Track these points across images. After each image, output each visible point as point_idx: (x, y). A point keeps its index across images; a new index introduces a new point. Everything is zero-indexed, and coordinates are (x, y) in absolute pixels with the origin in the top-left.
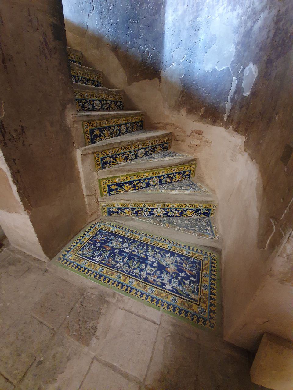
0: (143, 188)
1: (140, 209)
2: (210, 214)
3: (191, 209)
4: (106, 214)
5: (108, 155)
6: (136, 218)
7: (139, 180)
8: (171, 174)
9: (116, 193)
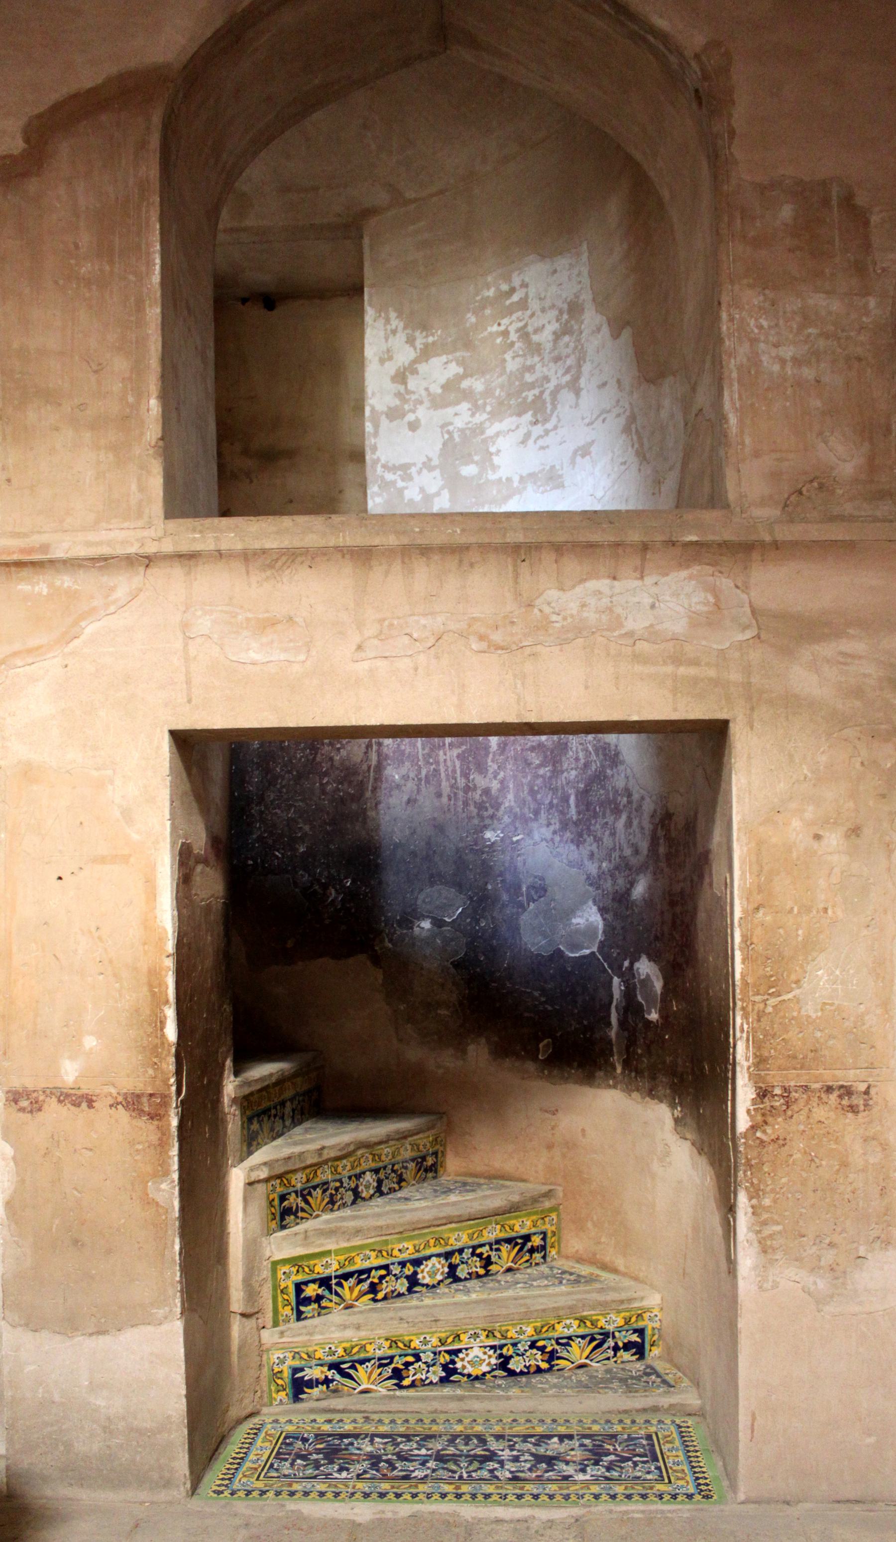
0: (400, 1295)
1: (410, 1359)
3: (583, 1337)
6: (398, 1393)
7: (386, 1267)
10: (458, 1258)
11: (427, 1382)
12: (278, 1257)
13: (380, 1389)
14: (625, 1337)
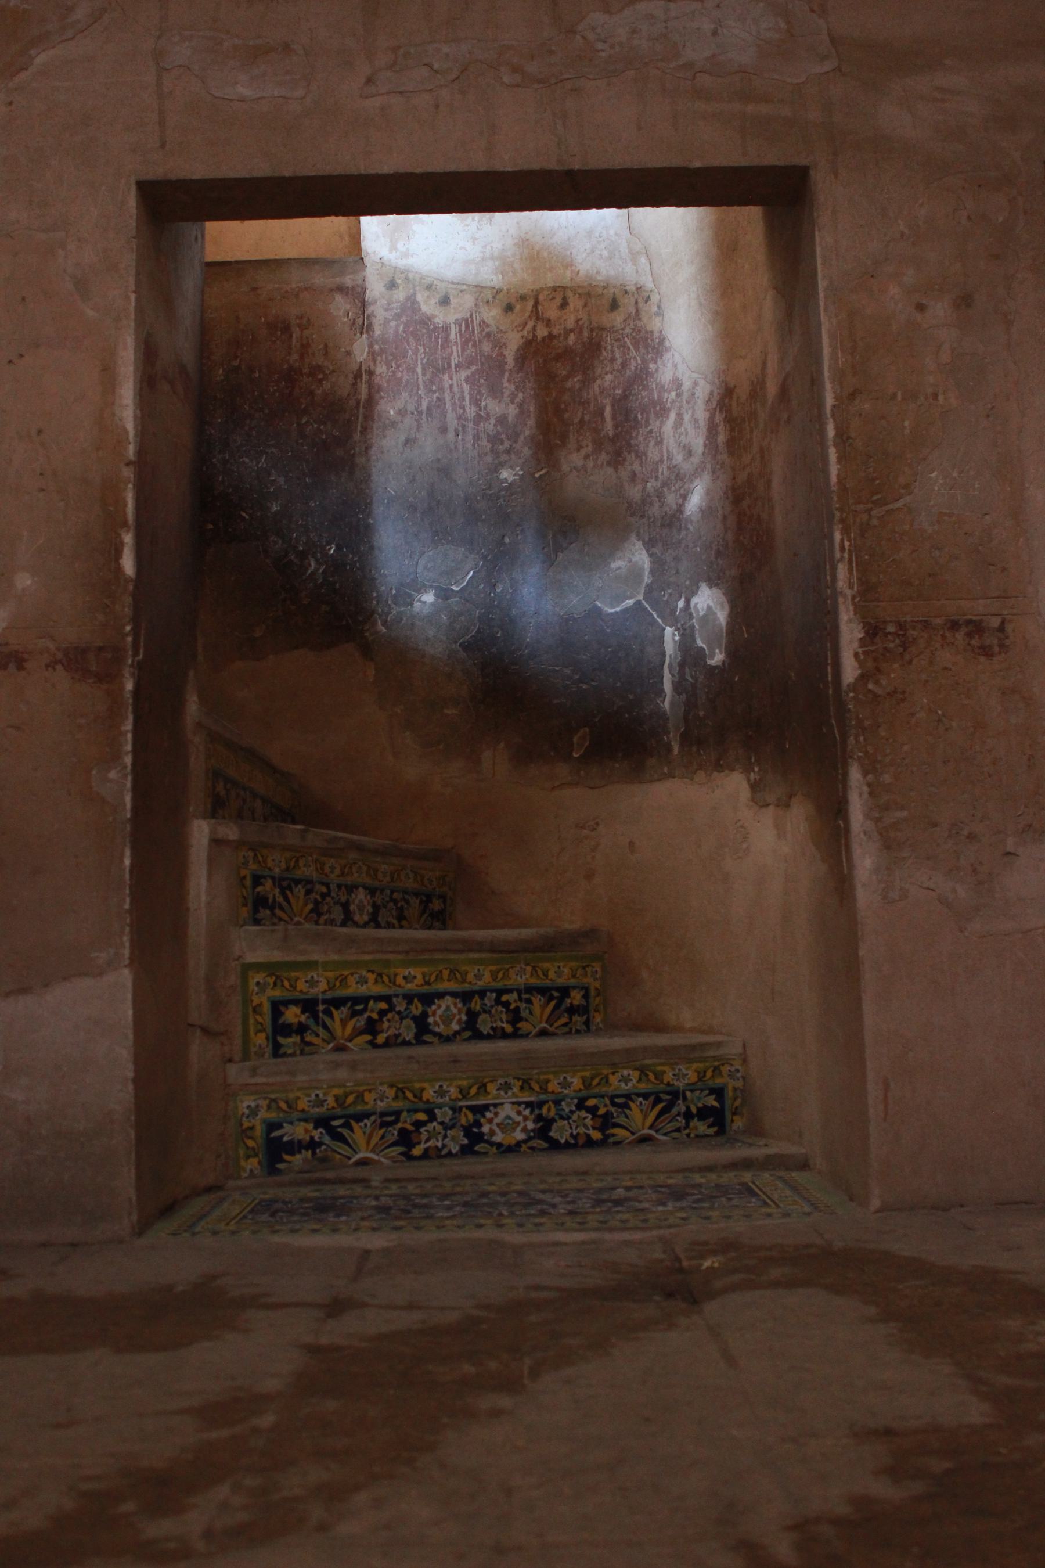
1: (422, 1116)
2: (728, 1115)
3: (645, 1096)
4: (254, 1162)
7: (387, 999)
9: (298, 1052)
10: (479, 1003)
11: (444, 1152)
12: (250, 958)
13: (383, 1160)
14: (699, 1099)
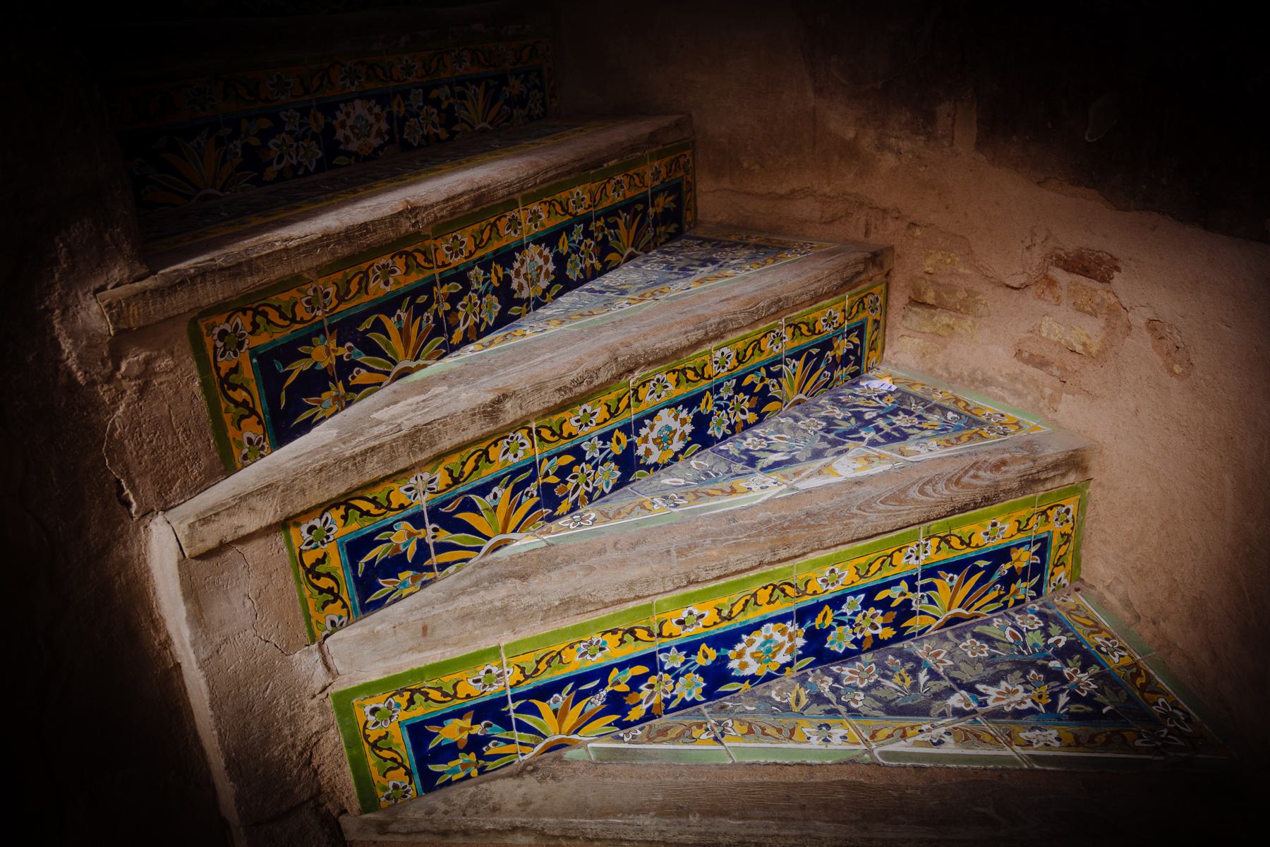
5: (402, 507)
7: (648, 659)
8: (896, 583)
9: (474, 772)
